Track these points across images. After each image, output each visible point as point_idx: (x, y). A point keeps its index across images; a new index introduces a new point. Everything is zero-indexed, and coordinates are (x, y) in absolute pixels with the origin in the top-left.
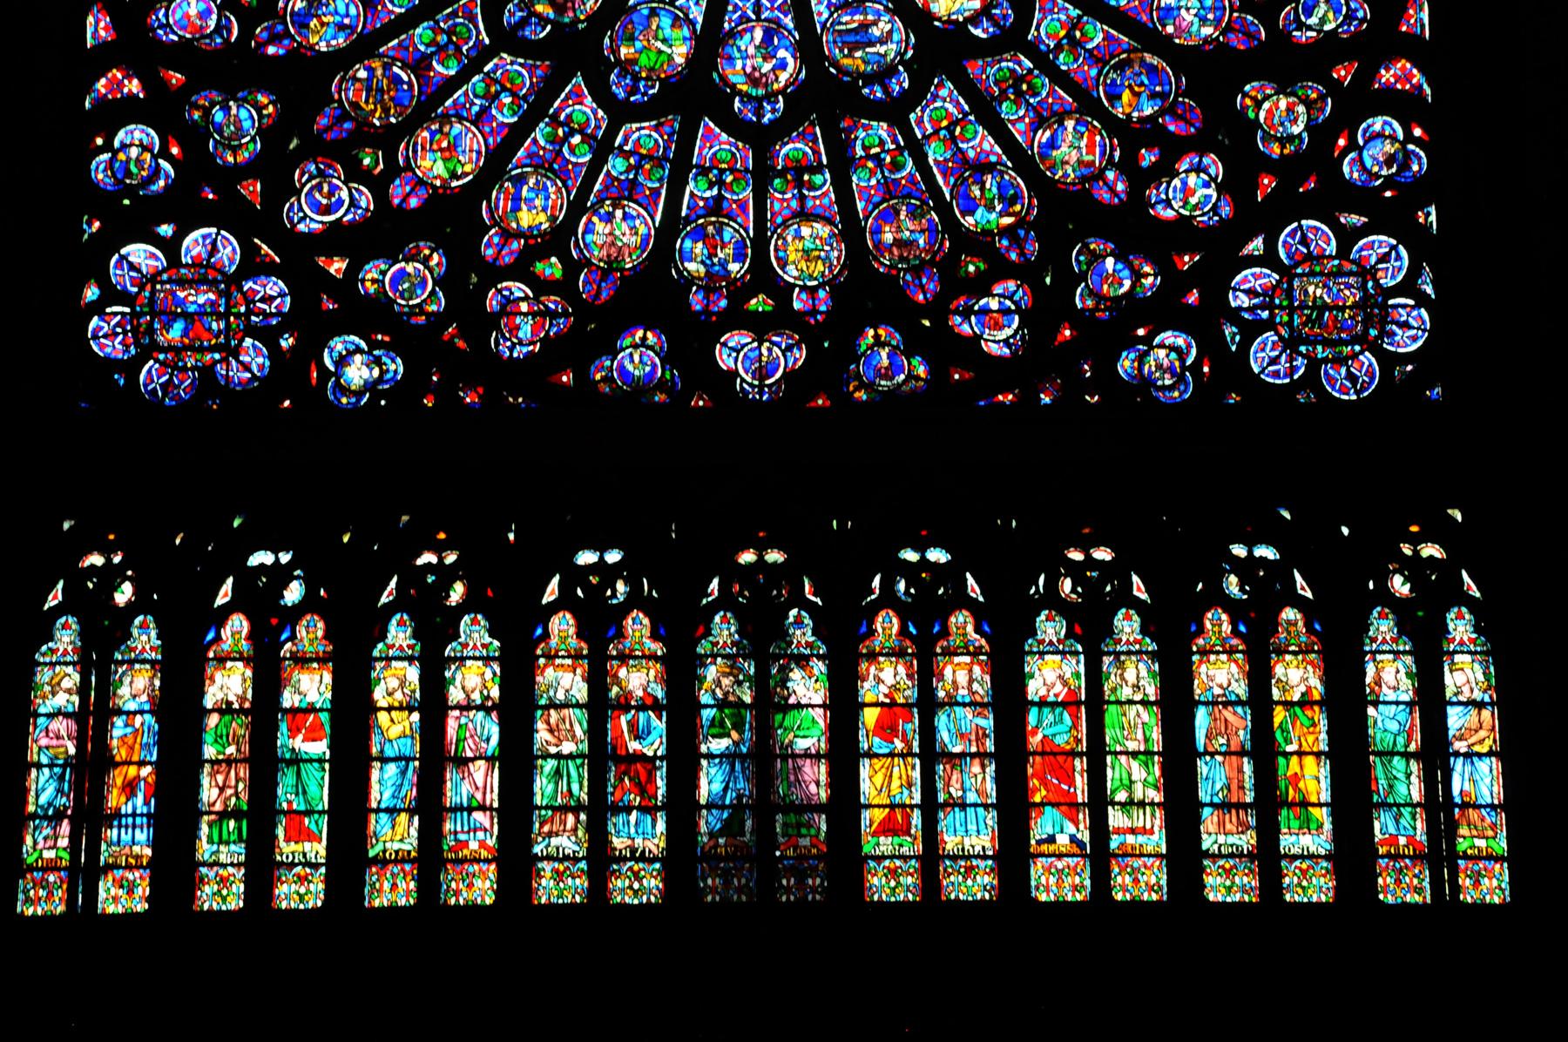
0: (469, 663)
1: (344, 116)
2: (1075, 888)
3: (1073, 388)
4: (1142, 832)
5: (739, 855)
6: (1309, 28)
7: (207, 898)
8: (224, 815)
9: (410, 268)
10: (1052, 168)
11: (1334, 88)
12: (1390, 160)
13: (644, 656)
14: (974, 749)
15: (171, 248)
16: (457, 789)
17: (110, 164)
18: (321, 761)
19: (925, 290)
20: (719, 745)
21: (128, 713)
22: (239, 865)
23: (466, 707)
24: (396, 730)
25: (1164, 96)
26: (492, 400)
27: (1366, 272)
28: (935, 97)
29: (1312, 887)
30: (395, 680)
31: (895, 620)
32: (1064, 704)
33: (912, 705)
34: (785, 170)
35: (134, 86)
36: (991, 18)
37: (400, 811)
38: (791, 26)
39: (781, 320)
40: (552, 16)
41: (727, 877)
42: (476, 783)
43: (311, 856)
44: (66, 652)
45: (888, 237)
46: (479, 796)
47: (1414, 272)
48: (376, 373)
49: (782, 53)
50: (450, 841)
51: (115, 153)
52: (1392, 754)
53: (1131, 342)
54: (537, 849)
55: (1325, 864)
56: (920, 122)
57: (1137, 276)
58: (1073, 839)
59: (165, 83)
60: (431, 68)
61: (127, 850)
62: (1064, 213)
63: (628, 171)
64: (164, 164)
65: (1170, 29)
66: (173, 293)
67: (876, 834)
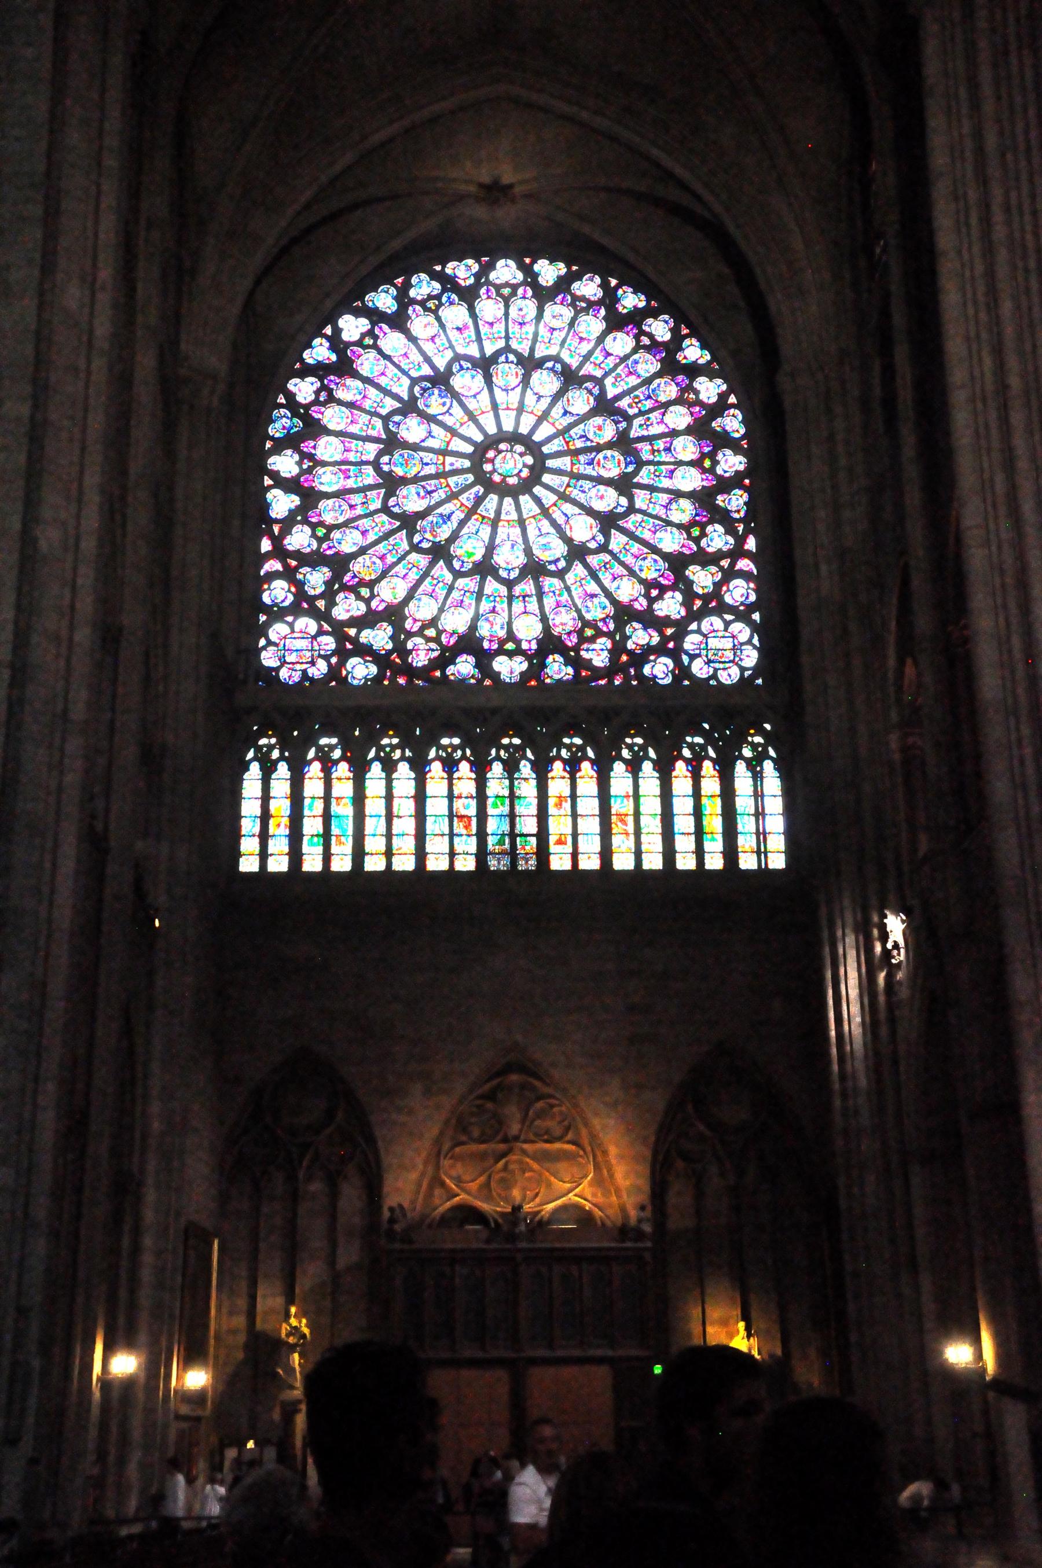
1: (355, 576)
3: (627, 679)
5: (503, 853)
11: (721, 568)
12: (742, 595)
15: (291, 625)
16: (398, 826)
19: (572, 641)
20: (497, 812)
24: (374, 806)
25: (659, 570)
26: (410, 681)
27: (733, 637)
34: (518, 597)
39: (519, 651)
40: (431, 538)
41: (499, 859)
47: (752, 637)
48: (365, 672)
53: (649, 661)
59: (289, 566)
62: (624, 614)
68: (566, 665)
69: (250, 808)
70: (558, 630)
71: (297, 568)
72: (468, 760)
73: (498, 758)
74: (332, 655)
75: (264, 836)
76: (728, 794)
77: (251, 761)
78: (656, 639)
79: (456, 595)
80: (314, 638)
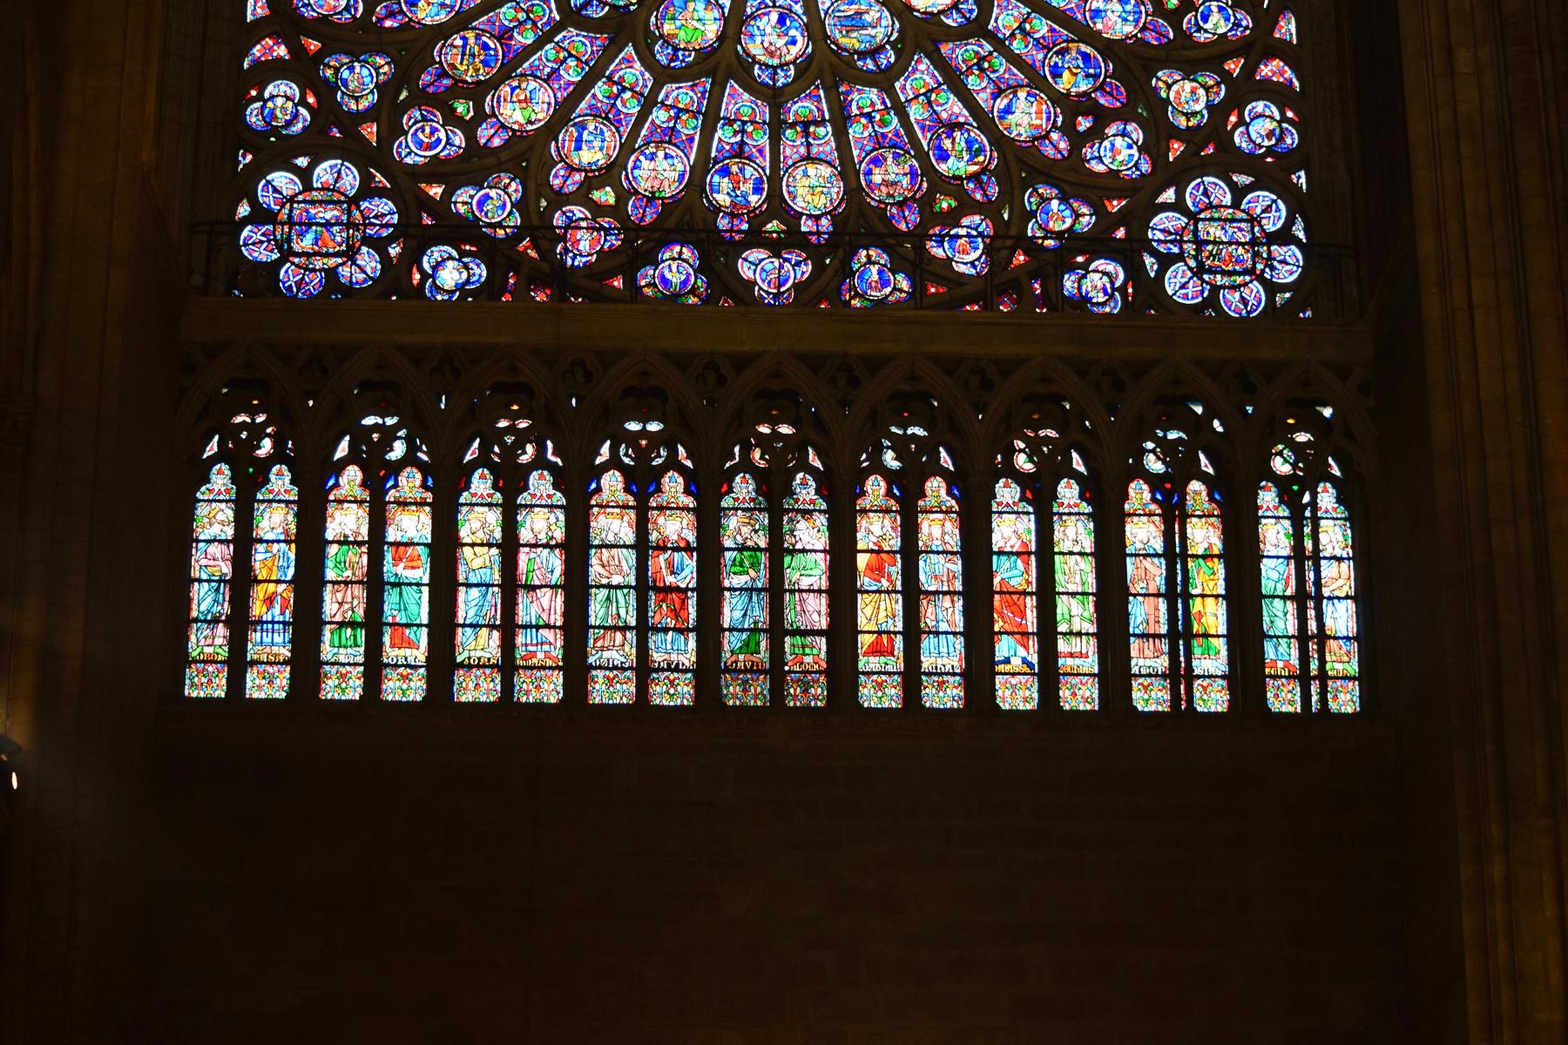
0: (536, 510)
1: (443, 74)
2: (1025, 700)
4: (1080, 655)
5: (754, 670)
6: (1206, 31)
7: (331, 690)
8: (342, 624)
9: (493, 193)
10: (1008, 128)
11: (1226, 77)
12: (1270, 134)
13: (678, 508)
14: (945, 588)
15: (305, 175)
16: (527, 609)
17: (263, 108)
18: (418, 585)
20: (739, 581)
21: (267, 542)
22: (355, 664)
23: (535, 546)
24: (478, 563)
25: (1096, 76)
26: (559, 297)
27: (1253, 220)
28: (915, 70)
29: (1213, 699)
30: (479, 522)
31: (883, 484)
32: (1018, 554)
33: (894, 552)
35: (282, 51)
36: (959, 11)
37: (482, 626)
38: (800, 11)
39: (793, 239)
42: (541, 607)
43: (411, 661)
44: (219, 493)
45: (877, 178)
46: (545, 616)
47: (1290, 222)
48: (465, 275)
49: (792, 32)
50: (520, 653)
51: (265, 101)
52: (1274, 597)
53: (1072, 268)
54: (591, 660)
55: (1220, 682)
56: (903, 88)
57: (1077, 216)
58: (1024, 661)
59: (305, 50)
60: (511, 38)
61: (268, 650)
62: (1019, 165)
63: (668, 121)
64: (302, 111)
65: (1099, 26)
66: (307, 211)
67: (866, 654)
68: (894, 272)
69: (210, 561)
70: (876, 195)
71: (319, 57)
72: (682, 470)
73: (746, 466)
74: (391, 239)
75: (240, 623)
76: (1241, 555)
77: (214, 460)
78: (1087, 221)
79: (660, 116)
80: (354, 201)
